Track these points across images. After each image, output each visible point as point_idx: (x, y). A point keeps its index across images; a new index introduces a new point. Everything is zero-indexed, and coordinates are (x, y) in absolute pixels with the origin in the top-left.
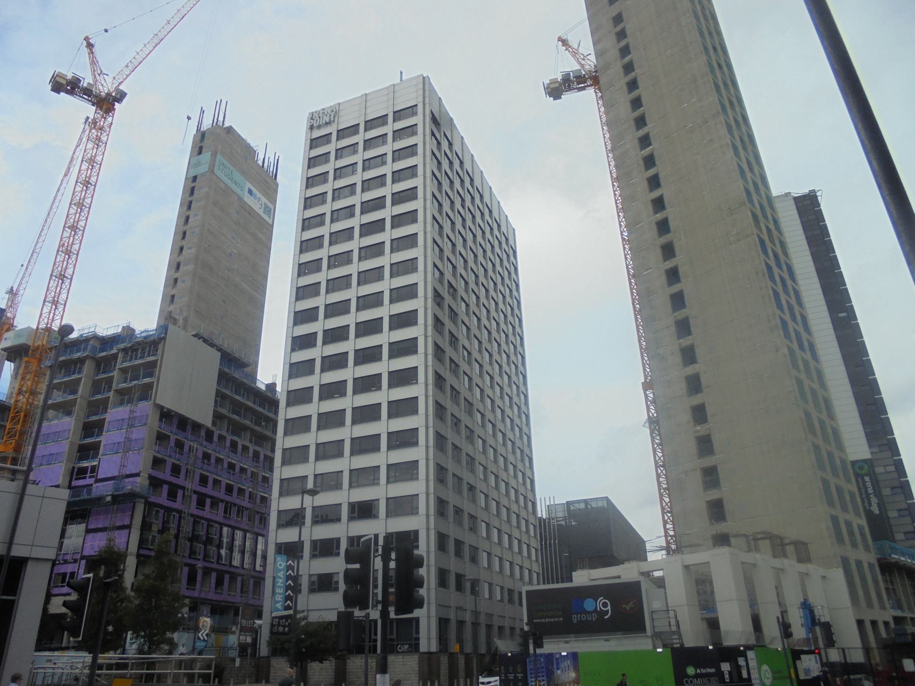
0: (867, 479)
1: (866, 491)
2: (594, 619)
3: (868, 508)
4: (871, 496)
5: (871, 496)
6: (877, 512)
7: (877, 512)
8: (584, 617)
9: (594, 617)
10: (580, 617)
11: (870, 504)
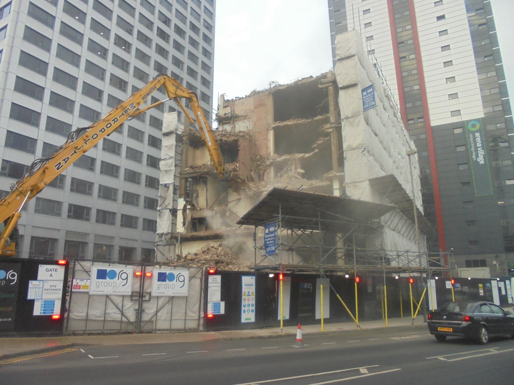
0: (477, 135)
3: (475, 159)
4: (479, 149)
5: (479, 149)
6: (482, 162)
7: (482, 162)
11: (477, 156)
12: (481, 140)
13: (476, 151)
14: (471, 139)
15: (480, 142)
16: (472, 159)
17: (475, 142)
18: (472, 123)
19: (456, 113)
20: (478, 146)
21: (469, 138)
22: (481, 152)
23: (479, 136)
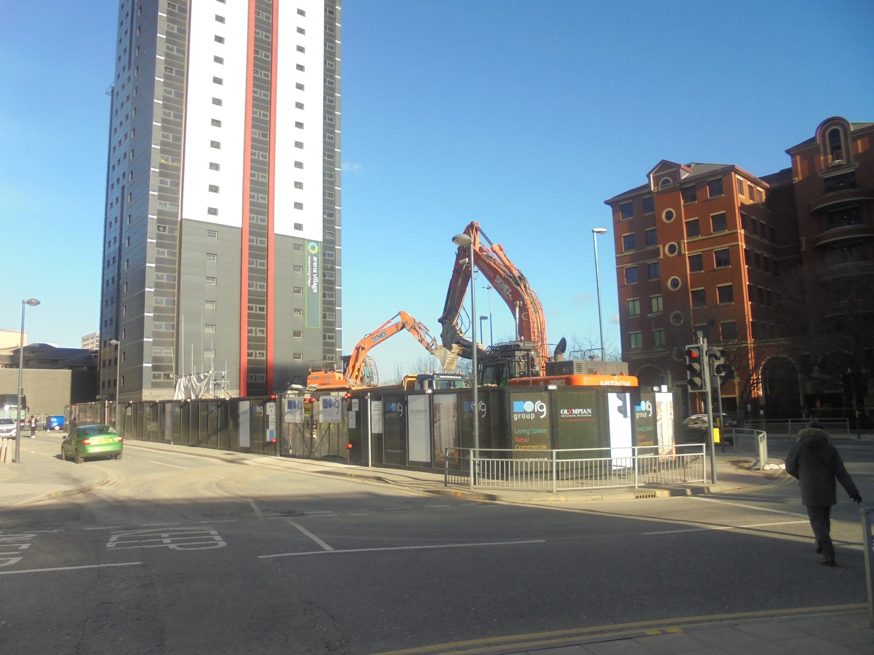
0: (315, 259)
1: (312, 270)
2: (532, 417)
4: (314, 275)
6: (315, 291)
8: (524, 417)
9: (533, 417)
10: (521, 416)
11: (312, 284)
12: (318, 266)
13: (312, 277)
14: (309, 262)
15: (316, 268)
16: (308, 284)
17: (312, 267)
18: (316, 246)
19: (298, 227)
20: (314, 272)
21: (308, 260)
22: (316, 280)
23: (316, 261)
